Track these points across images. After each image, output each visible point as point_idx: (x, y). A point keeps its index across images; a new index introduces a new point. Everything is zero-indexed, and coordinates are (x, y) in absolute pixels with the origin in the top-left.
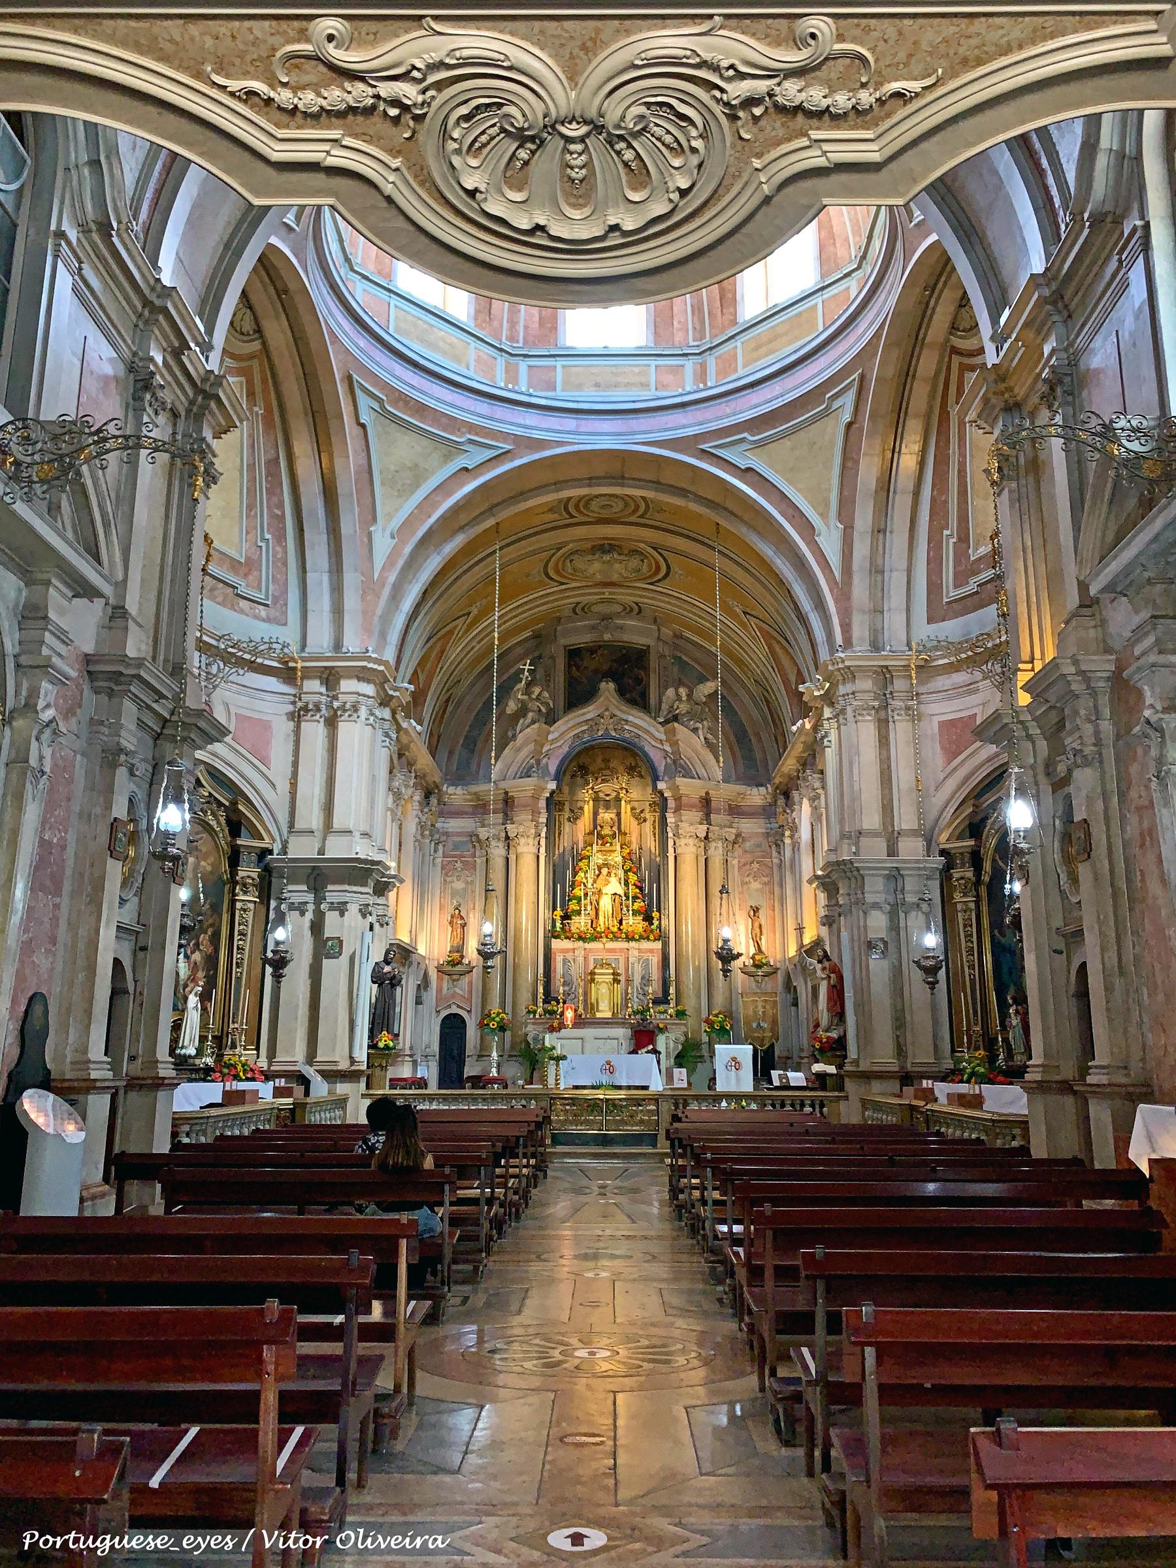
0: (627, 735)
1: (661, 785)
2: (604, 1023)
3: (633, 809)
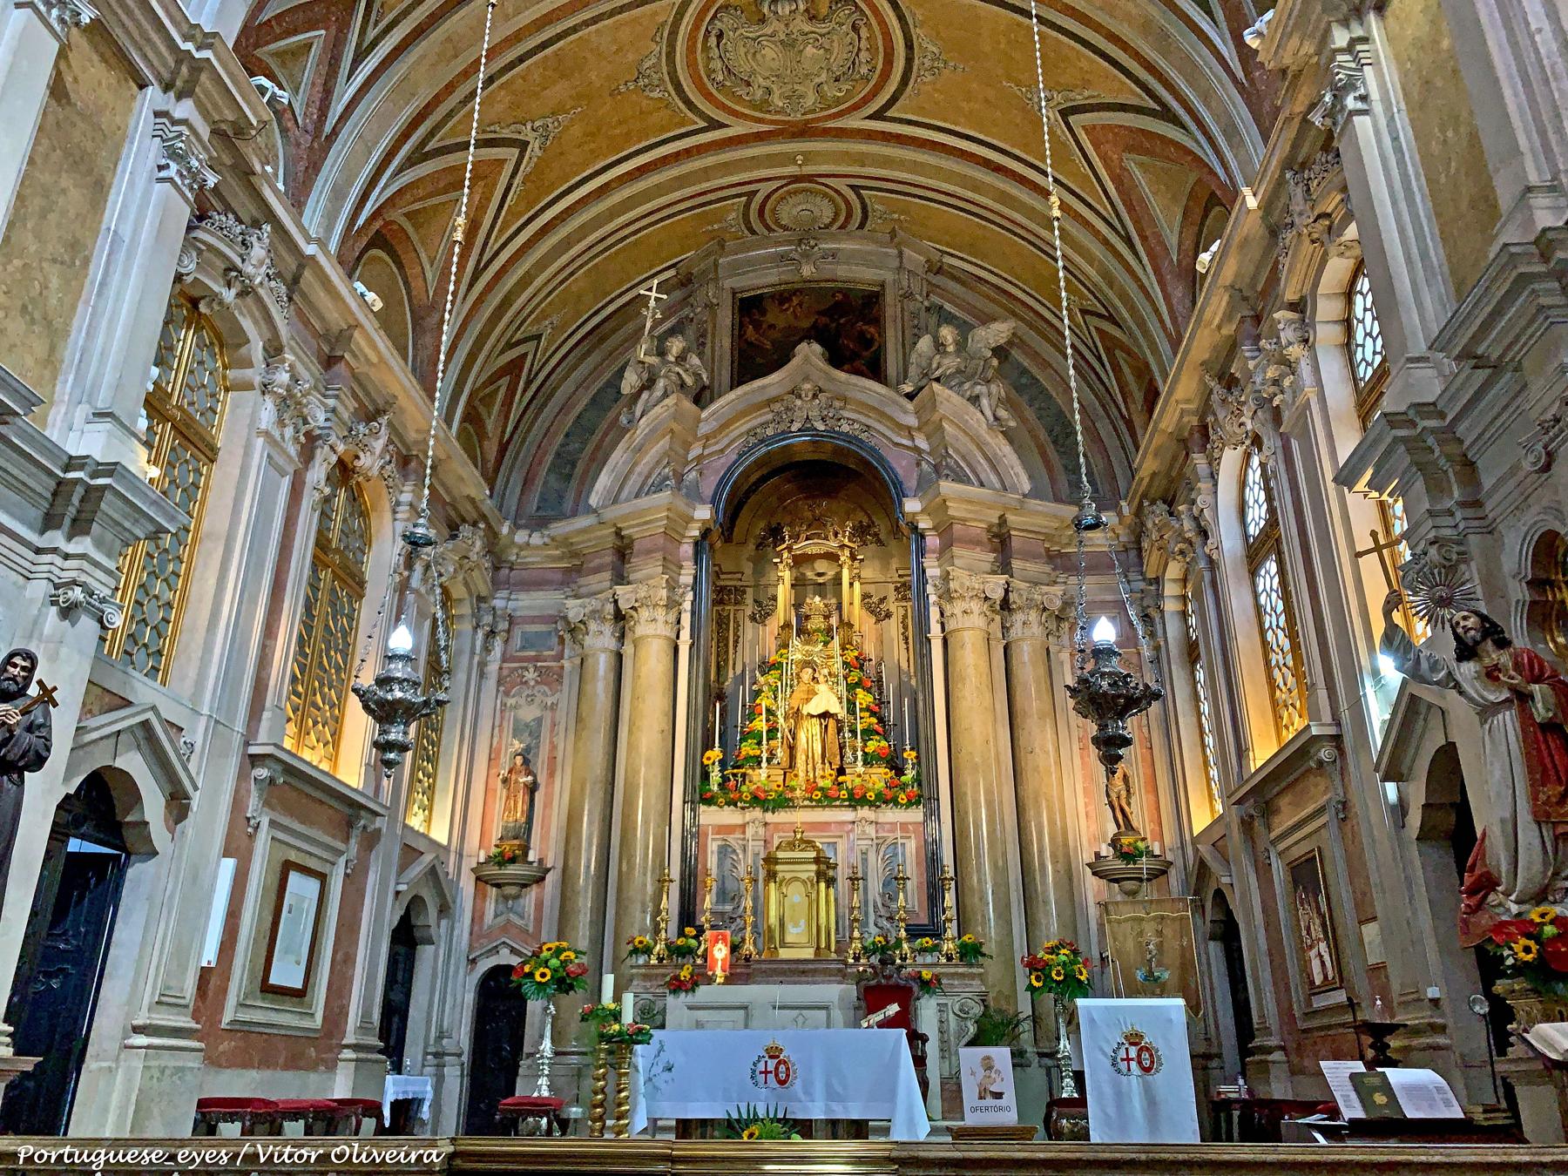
0: (845, 428)
2: (797, 972)
3: (865, 596)
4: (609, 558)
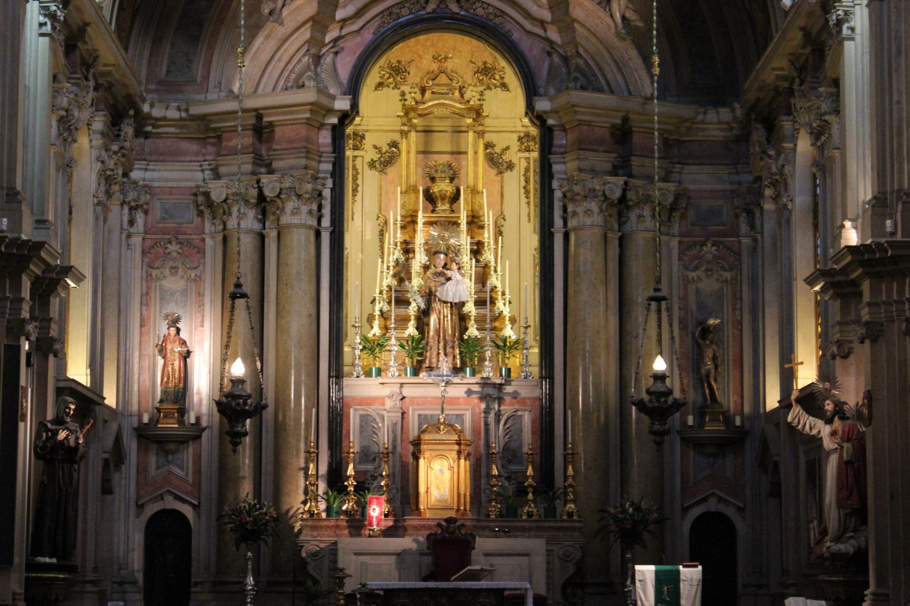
1: (542, 105)
3: (488, 145)
4: (248, 139)
